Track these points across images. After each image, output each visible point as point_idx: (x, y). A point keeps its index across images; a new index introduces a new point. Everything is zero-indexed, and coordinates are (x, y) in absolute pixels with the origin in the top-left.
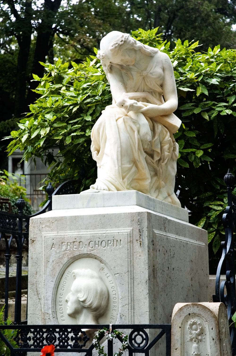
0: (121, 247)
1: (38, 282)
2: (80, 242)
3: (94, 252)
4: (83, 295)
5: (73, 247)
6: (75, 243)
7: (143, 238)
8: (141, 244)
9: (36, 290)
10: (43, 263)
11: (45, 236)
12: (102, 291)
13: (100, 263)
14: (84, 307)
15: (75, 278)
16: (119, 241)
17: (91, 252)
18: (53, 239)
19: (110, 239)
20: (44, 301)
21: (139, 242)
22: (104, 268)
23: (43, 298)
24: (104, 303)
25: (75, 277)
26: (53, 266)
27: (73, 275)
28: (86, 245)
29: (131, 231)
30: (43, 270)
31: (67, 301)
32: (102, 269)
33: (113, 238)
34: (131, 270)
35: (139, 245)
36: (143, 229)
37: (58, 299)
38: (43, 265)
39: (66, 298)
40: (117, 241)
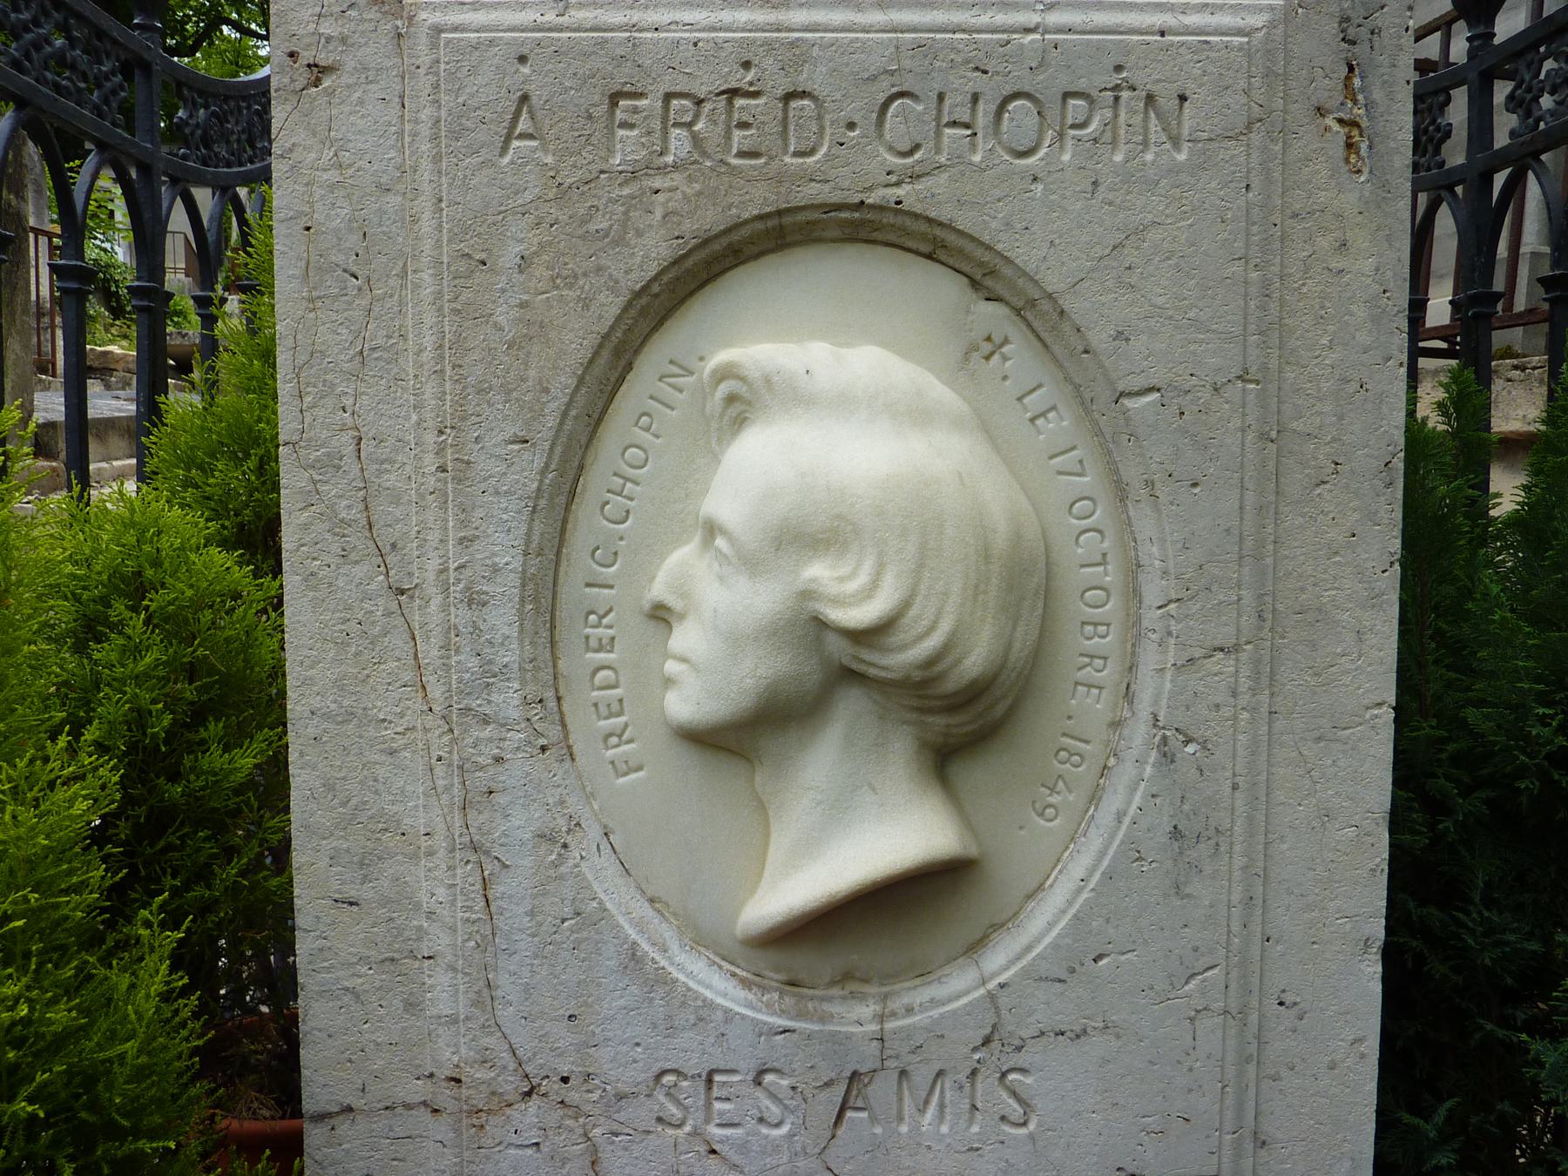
0: (1182, 157)
1: (378, 440)
2: (789, 97)
3: (932, 196)
4: (862, 579)
5: (728, 136)
6: (740, 102)
7: (1377, 95)
8: (1349, 146)
9: (355, 513)
10: (426, 276)
11: (438, 30)
12: (1017, 538)
13: (969, 291)
14: (849, 675)
15: (740, 423)
16: (1168, 103)
17: (900, 192)
18: (522, 59)
19: (1082, 85)
20: (445, 608)
21: (1336, 127)
22: (1006, 341)
23: (432, 590)
24: (1024, 637)
25: (740, 404)
26: (523, 305)
27: (724, 389)
28: (851, 126)
29: (1271, 25)
30: (429, 341)
31: (661, 615)
32: (987, 347)
33: (1116, 79)
34: (1264, 368)
35: (1340, 151)
36: (1379, 19)
37: (572, 590)
38: (427, 292)
39: (659, 590)
40: (1150, 99)
